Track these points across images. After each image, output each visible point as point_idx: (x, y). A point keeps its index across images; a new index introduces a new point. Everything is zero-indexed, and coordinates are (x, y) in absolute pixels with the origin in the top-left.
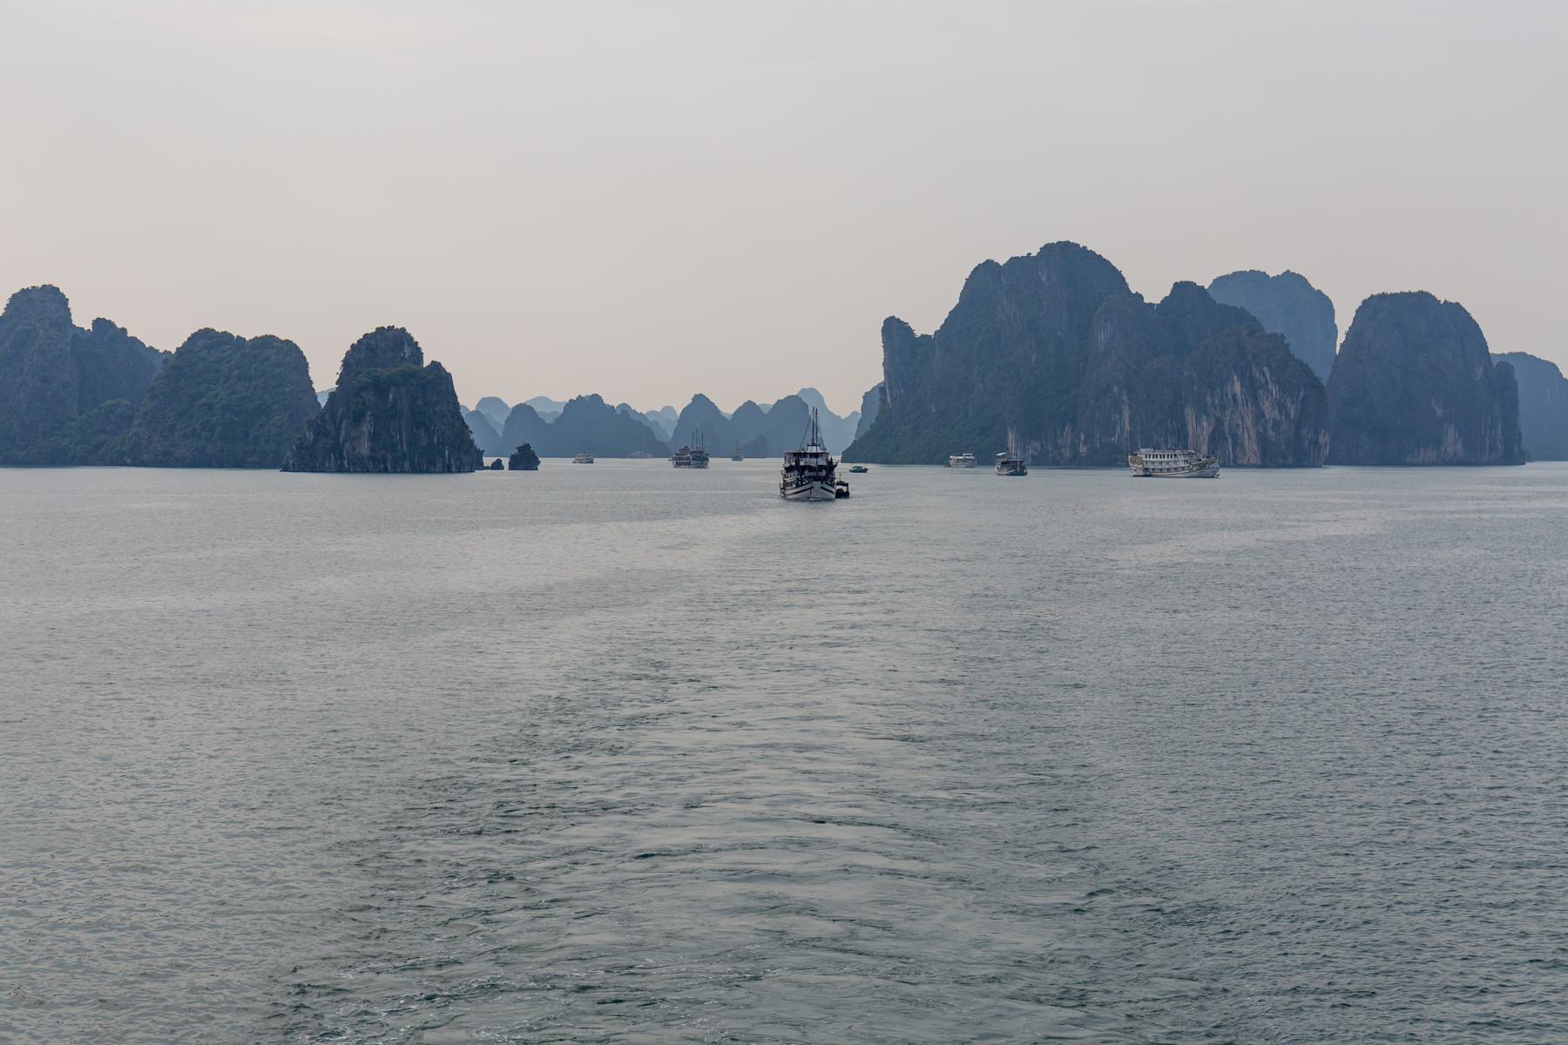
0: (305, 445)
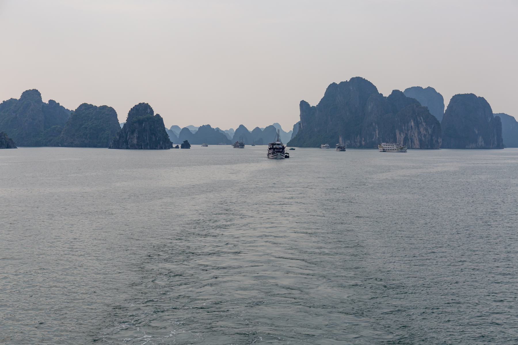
0: (116, 140)
